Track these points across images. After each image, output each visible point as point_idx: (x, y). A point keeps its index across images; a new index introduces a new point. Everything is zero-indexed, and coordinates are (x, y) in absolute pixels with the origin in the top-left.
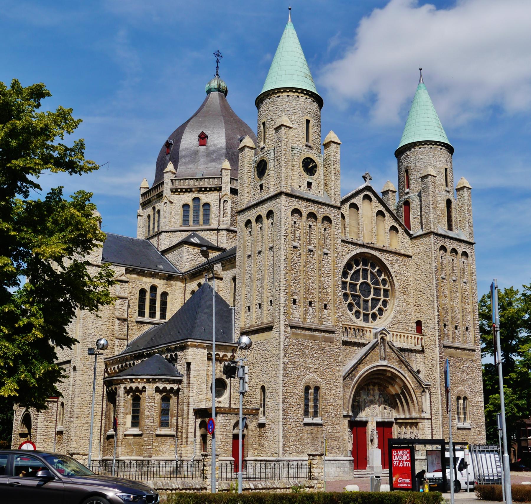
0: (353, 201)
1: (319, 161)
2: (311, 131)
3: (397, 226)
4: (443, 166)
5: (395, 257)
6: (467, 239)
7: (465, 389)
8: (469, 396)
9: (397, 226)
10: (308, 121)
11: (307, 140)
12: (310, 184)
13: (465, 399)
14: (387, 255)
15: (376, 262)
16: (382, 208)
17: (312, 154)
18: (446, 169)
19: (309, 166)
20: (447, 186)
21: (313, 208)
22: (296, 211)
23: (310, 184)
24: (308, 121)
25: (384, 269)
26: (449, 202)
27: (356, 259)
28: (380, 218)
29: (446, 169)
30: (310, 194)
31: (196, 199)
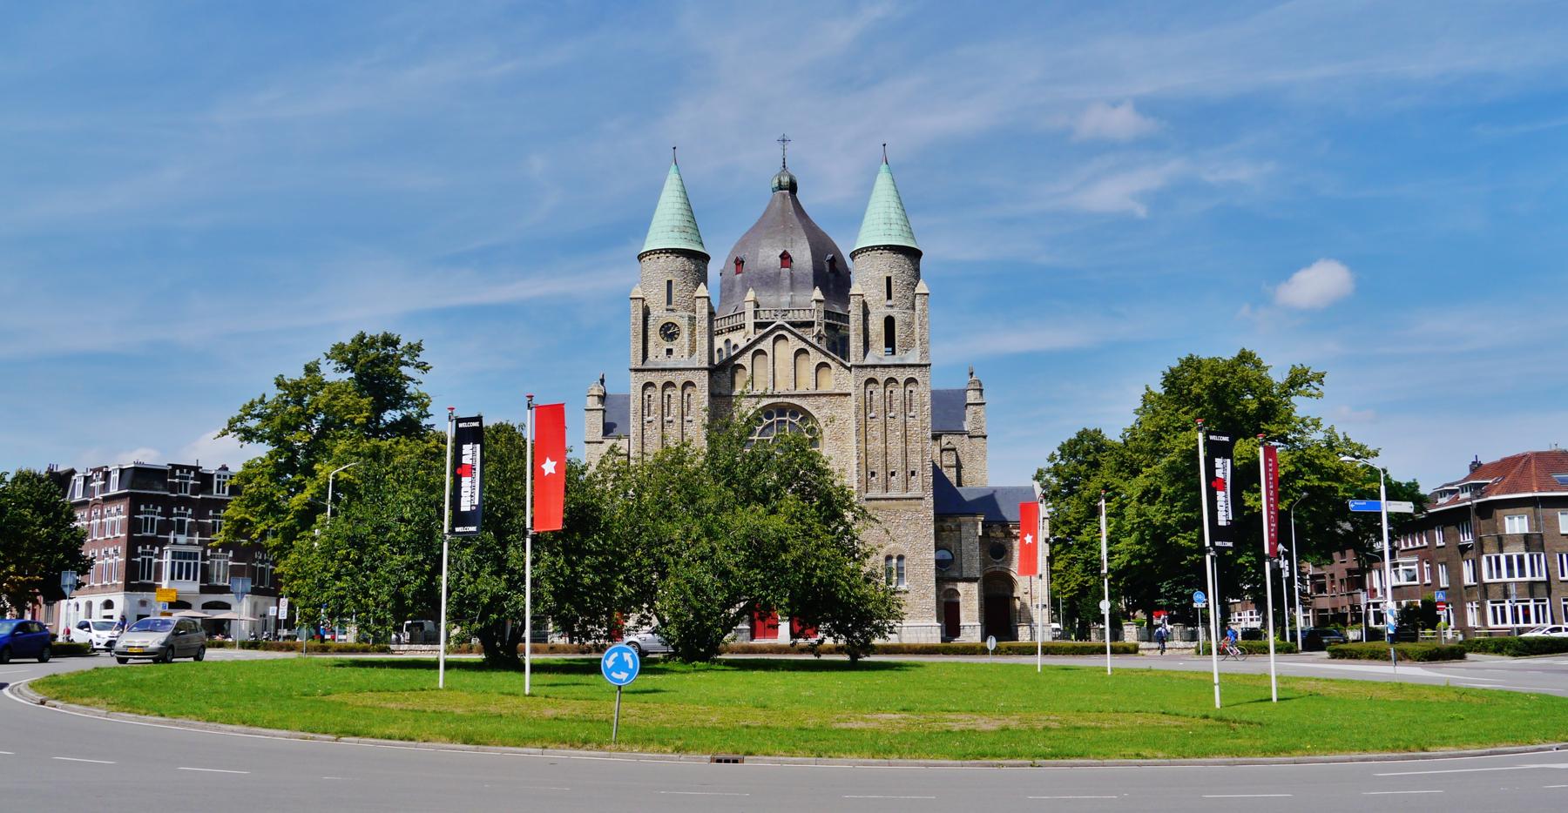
0: (758, 347)
1: (683, 323)
2: (674, 292)
3: (829, 361)
4: (883, 276)
5: (824, 399)
6: (917, 362)
7: (902, 546)
8: (907, 553)
9: (829, 361)
10: (670, 283)
11: (669, 302)
12: (669, 352)
13: (901, 558)
14: (810, 400)
15: (796, 411)
16: (803, 345)
17: (671, 317)
18: (889, 279)
19: (669, 332)
20: (889, 297)
21: (669, 377)
22: (649, 385)
23: (669, 352)
24: (670, 283)
25: (807, 416)
26: (889, 322)
27: (767, 412)
28: (802, 357)
29: (889, 279)
30: (670, 363)
31: (727, 341)
